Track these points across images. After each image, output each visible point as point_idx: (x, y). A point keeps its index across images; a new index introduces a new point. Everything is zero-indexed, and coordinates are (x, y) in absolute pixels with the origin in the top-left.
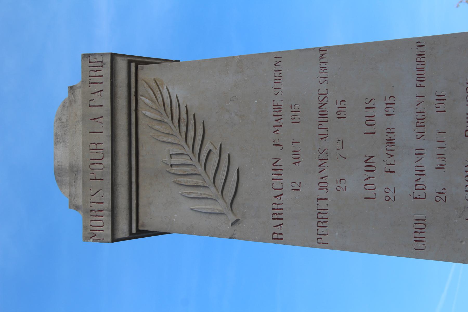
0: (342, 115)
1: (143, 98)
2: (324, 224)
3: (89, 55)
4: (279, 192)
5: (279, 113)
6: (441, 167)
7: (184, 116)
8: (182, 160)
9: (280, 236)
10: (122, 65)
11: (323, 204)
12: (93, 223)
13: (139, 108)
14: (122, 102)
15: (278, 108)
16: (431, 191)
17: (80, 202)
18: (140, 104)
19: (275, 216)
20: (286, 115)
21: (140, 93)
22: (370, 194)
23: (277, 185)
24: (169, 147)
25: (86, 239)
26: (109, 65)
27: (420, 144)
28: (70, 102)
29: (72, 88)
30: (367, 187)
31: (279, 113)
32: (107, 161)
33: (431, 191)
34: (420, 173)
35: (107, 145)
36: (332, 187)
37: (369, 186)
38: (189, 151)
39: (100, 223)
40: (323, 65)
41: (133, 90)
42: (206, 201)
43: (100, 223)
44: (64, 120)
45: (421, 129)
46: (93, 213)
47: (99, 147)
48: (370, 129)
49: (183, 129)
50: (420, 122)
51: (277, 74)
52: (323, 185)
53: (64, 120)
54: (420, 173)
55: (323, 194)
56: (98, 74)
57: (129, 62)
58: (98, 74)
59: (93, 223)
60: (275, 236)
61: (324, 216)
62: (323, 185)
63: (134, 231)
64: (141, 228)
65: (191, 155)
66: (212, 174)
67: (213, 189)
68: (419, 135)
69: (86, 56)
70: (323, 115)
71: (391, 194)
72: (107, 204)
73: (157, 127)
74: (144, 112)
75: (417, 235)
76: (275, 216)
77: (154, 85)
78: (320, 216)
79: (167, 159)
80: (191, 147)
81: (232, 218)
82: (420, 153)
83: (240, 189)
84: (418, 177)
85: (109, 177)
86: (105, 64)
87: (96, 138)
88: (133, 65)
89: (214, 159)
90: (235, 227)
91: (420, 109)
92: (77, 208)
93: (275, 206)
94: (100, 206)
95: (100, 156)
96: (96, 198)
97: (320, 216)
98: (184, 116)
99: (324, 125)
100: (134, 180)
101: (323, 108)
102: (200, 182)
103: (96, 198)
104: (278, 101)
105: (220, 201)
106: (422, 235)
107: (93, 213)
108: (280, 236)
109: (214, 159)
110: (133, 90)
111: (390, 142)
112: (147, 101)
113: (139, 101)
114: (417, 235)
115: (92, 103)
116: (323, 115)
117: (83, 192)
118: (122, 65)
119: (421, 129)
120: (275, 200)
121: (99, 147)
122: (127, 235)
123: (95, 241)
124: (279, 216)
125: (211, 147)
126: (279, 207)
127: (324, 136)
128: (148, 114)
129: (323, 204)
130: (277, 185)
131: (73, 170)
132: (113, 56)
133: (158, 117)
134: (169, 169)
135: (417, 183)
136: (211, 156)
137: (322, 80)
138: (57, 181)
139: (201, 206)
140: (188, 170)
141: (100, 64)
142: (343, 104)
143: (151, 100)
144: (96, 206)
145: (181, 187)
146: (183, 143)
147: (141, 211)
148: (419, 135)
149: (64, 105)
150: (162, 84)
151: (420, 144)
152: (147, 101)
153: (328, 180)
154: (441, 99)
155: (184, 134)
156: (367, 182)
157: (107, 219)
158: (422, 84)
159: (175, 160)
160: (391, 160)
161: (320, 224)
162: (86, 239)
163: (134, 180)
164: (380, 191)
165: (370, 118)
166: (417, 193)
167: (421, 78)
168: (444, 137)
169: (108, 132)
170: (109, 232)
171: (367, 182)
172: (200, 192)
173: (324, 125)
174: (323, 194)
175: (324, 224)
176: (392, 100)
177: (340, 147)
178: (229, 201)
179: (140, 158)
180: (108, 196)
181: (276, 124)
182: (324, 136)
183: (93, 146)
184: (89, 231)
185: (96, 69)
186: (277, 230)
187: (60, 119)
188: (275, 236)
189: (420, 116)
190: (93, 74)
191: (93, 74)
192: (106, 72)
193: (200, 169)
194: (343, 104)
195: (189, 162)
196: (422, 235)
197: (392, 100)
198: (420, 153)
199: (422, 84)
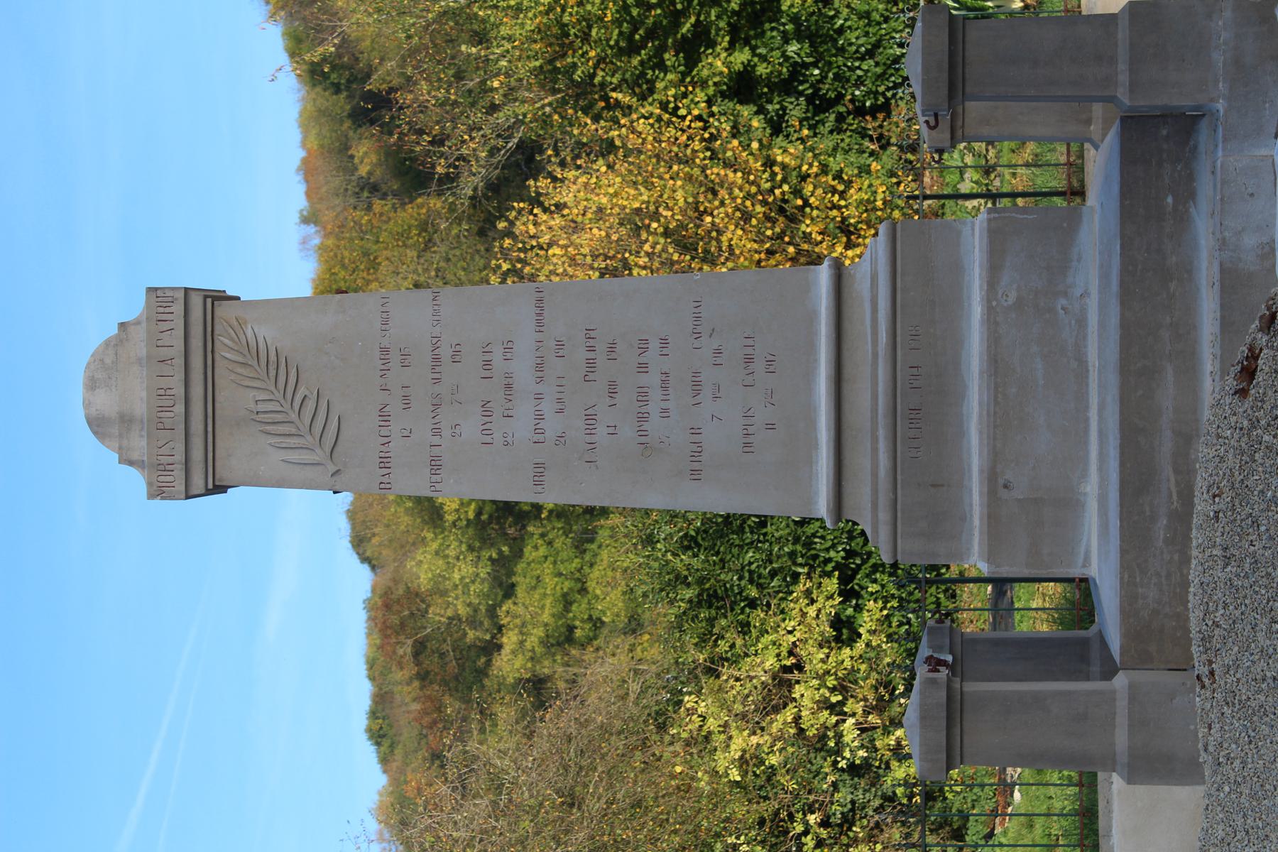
0: (457, 359)
1: (222, 338)
2: (438, 472)
3: (156, 289)
4: (386, 440)
5: (387, 357)
6: (561, 411)
7: (273, 357)
8: (270, 407)
9: (388, 486)
10: (196, 301)
11: (436, 451)
12: (161, 479)
13: (216, 349)
14: (196, 343)
15: (385, 350)
16: (550, 434)
17: (135, 456)
18: (217, 344)
19: (382, 465)
20: (395, 358)
21: (216, 332)
22: (488, 439)
23: (384, 432)
24: (254, 393)
25: (151, 496)
26: (182, 301)
27: (540, 388)
28: (121, 341)
29: (122, 326)
30: (484, 432)
31: (387, 357)
32: (180, 408)
33: (550, 434)
34: (540, 417)
35: (180, 391)
36: (446, 433)
37: (486, 431)
38: (279, 396)
39: (171, 479)
40: (436, 307)
41: (209, 329)
42: (301, 451)
43: (171, 479)
44: (108, 361)
45: (540, 374)
46: (162, 467)
47: (169, 392)
48: (487, 374)
49: (272, 373)
50: (539, 367)
51: (384, 315)
52: (437, 432)
53: (108, 361)
54: (540, 417)
55: (436, 440)
56: (167, 310)
57: (206, 297)
58: (167, 310)
59: (161, 479)
60: (382, 486)
61: (438, 463)
62: (437, 432)
63: (210, 486)
64: (217, 483)
65: (282, 401)
66: (307, 421)
67: (309, 438)
68: (538, 380)
69: (151, 290)
70: (437, 359)
71: (509, 439)
72: (179, 457)
73: (240, 370)
74: (221, 352)
75: (536, 478)
76: (382, 465)
77: (236, 323)
78: (433, 463)
79: (252, 406)
80: (282, 392)
81: (332, 468)
82: (539, 397)
83: (341, 438)
84: (537, 421)
85: (183, 426)
86: (176, 299)
87: (164, 383)
88: (209, 300)
89: (310, 405)
90: (335, 478)
91: (538, 354)
92: (131, 463)
93: (382, 455)
94: (170, 459)
95: (170, 403)
96: (164, 450)
97: (433, 463)
98: (273, 357)
99: (438, 369)
100: (210, 429)
101: (436, 352)
102: (294, 431)
103: (164, 450)
104: (385, 343)
105: (318, 451)
106: (541, 479)
107: (162, 467)
108: (388, 486)
109: (310, 405)
110: (209, 329)
111: (508, 387)
112: (226, 341)
113: (216, 342)
114: (536, 478)
115: (160, 343)
116: (437, 359)
117: (148, 444)
118: (196, 301)
119: (540, 374)
120: (383, 448)
121: (169, 392)
122: (203, 491)
123: (163, 498)
124: (387, 465)
125: (307, 393)
126: (387, 455)
127: (437, 381)
128: (228, 355)
129: (436, 451)
130: (384, 432)
131: (126, 420)
132: (186, 290)
133: (240, 359)
134: (255, 417)
135: (538, 427)
136: (307, 400)
137: (435, 323)
138: (95, 433)
139: (294, 456)
140: (279, 417)
141: (170, 299)
142: (458, 348)
143: (232, 339)
144: (165, 460)
145: (269, 436)
146: (273, 388)
147: (217, 464)
148: (538, 380)
149: (107, 343)
150: (246, 323)
151: (540, 388)
152: (226, 341)
153: (441, 425)
154: (560, 344)
155: (273, 379)
156: (485, 427)
157: (179, 473)
158: (542, 329)
159: (261, 407)
160: (509, 405)
161: (433, 472)
162: (151, 496)
163: (210, 429)
164: (498, 436)
165: (487, 363)
166: (537, 437)
167: (539, 323)
168: (563, 382)
169: (180, 376)
170: (183, 488)
171: (485, 427)
172: (293, 441)
173: (438, 369)
174: (436, 440)
175: (438, 472)
176: (510, 345)
177: (455, 392)
178: (328, 450)
179: (217, 405)
180: (180, 447)
181: (383, 367)
182: (437, 381)
183: (162, 392)
184: (155, 488)
185: (165, 304)
186: (385, 479)
187: (102, 360)
188: (382, 486)
189: (539, 361)
190: (161, 310)
191: (161, 310)
192: (178, 308)
193: (294, 416)
194: (458, 348)
195: (280, 409)
196: (541, 479)
197: (510, 345)
198: (539, 397)
199: (542, 329)
